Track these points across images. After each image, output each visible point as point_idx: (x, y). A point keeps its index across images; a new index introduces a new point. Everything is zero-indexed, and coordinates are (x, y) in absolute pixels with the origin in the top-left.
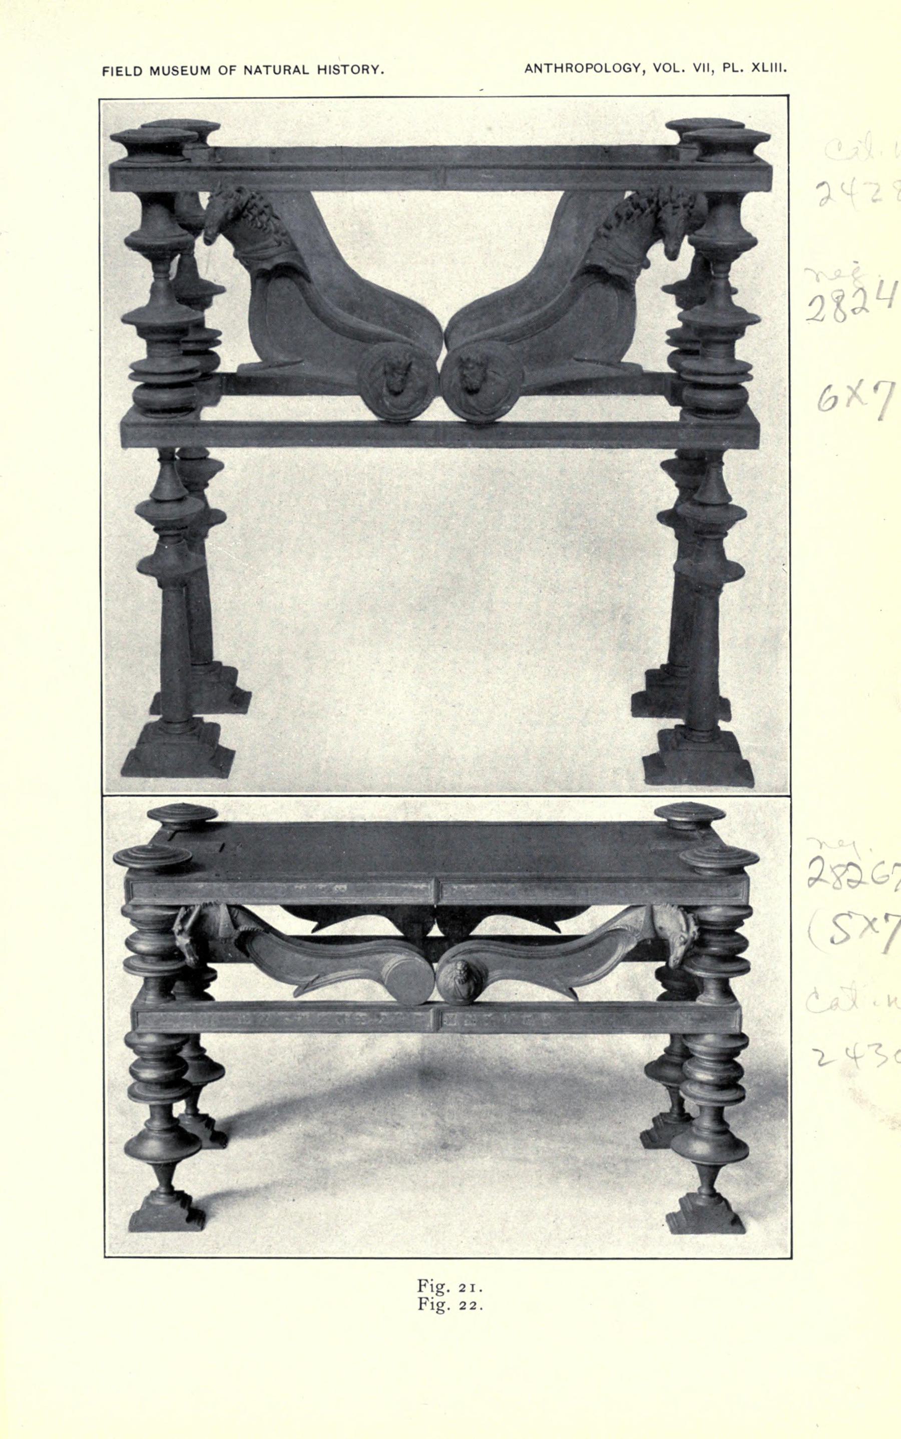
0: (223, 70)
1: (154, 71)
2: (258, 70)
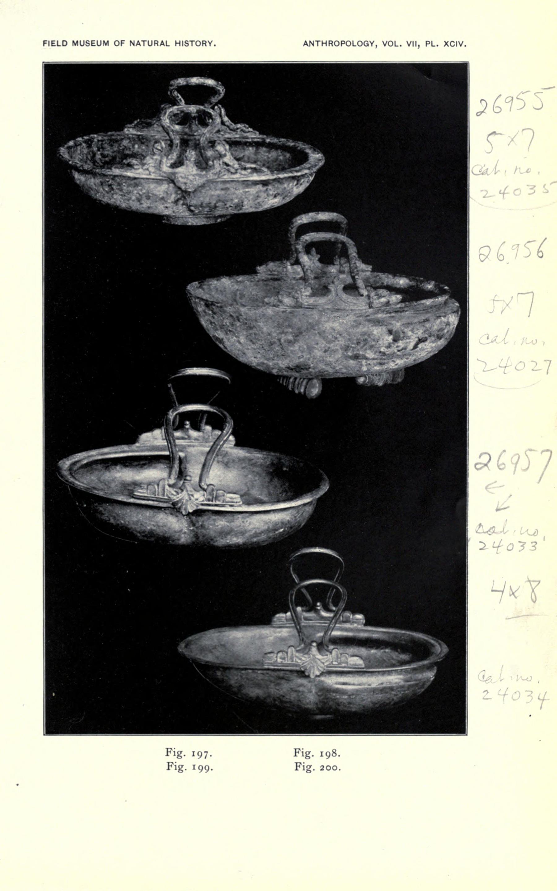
0: (117, 43)
1: (75, 43)
2: (139, 43)
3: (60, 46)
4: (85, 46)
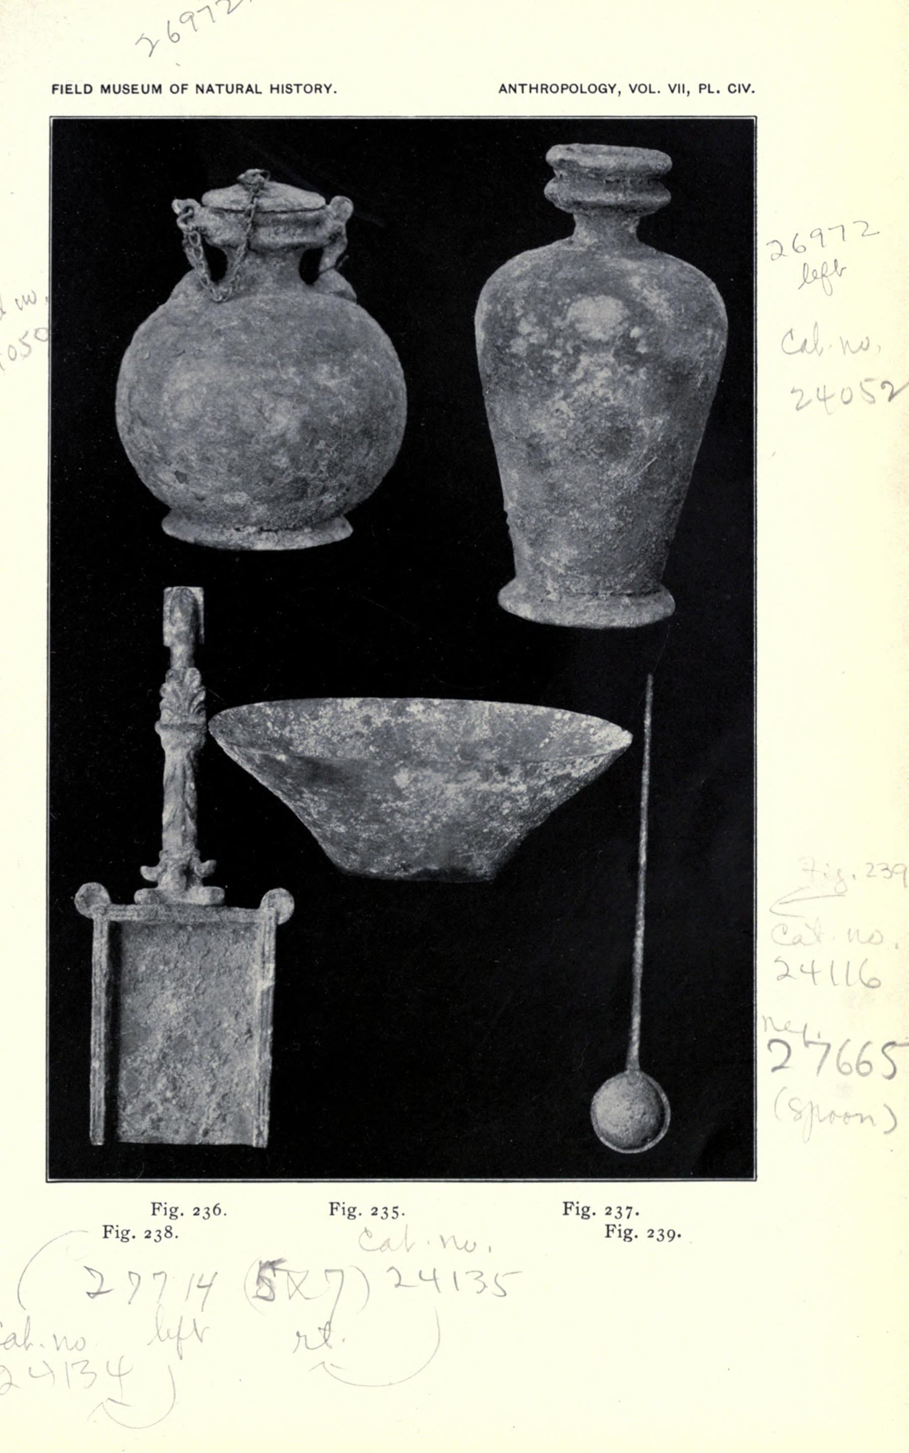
1: (105, 89)
2: (210, 89)
3: (80, 93)
4: (121, 92)
